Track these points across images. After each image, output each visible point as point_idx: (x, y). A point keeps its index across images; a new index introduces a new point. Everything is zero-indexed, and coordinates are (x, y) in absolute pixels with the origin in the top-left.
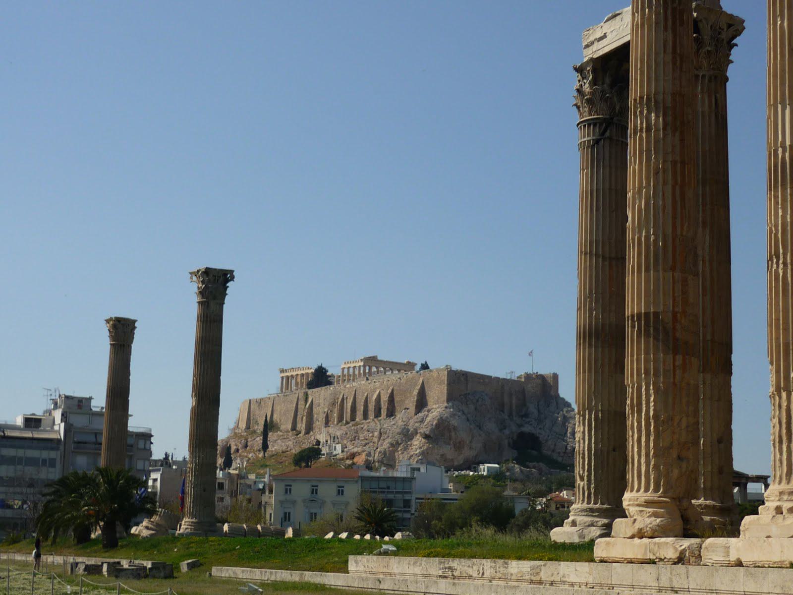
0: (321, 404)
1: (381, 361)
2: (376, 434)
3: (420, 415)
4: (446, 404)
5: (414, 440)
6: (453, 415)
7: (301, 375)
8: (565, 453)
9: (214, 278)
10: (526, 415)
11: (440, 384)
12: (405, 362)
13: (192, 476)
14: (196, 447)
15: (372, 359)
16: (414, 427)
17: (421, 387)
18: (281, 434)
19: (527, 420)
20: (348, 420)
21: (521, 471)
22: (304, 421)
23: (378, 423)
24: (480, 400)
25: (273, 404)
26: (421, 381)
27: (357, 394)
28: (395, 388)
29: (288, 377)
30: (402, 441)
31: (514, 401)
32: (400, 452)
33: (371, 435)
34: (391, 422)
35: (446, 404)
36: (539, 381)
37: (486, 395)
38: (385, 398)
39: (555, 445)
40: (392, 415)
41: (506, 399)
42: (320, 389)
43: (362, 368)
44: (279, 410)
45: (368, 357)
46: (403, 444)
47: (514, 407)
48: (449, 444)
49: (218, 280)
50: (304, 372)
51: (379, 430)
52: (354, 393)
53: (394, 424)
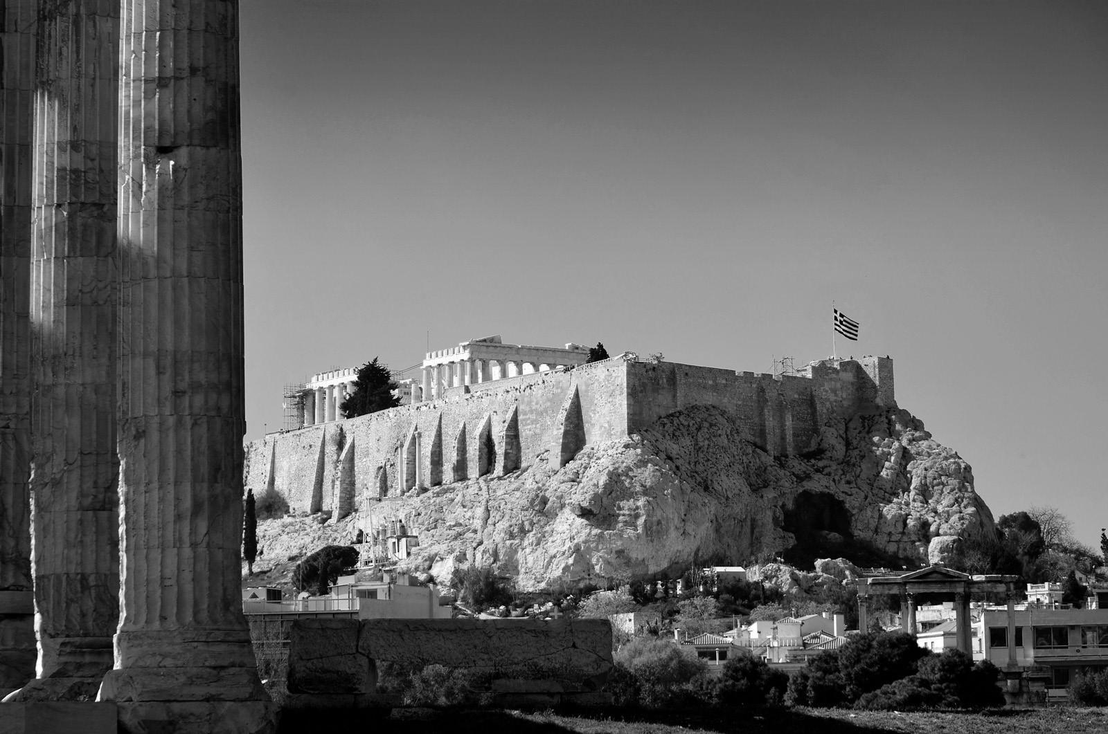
0: (371, 451)
1: (510, 348)
2: (480, 511)
3: (571, 465)
5: (558, 521)
6: (642, 463)
7: (339, 386)
8: (903, 533)
10: (819, 453)
12: (567, 346)
15: (489, 344)
16: (558, 494)
18: (290, 520)
19: (821, 464)
20: (427, 484)
21: (795, 580)
22: (337, 491)
23: (485, 488)
24: (706, 425)
25: (274, 454)
26: (571, 393)
27: (443, 426)
28: (521, 408)
30: (532, 524)
31: (789, 423)
32: (528, 550)
33: (469, 514)
34: (511, 483)
35: (626, 439)
36: (849, 376)
37: (723, 413)
38: (498, 434)
40: (517, 467)
41: (771, 423)
42: (367, 416)
43: (468, 365)
45: (480, 341)
46: (534, 532)
47: (789, 438)
51: (484, 502)
52: (437, 423)
53: (517, 489)
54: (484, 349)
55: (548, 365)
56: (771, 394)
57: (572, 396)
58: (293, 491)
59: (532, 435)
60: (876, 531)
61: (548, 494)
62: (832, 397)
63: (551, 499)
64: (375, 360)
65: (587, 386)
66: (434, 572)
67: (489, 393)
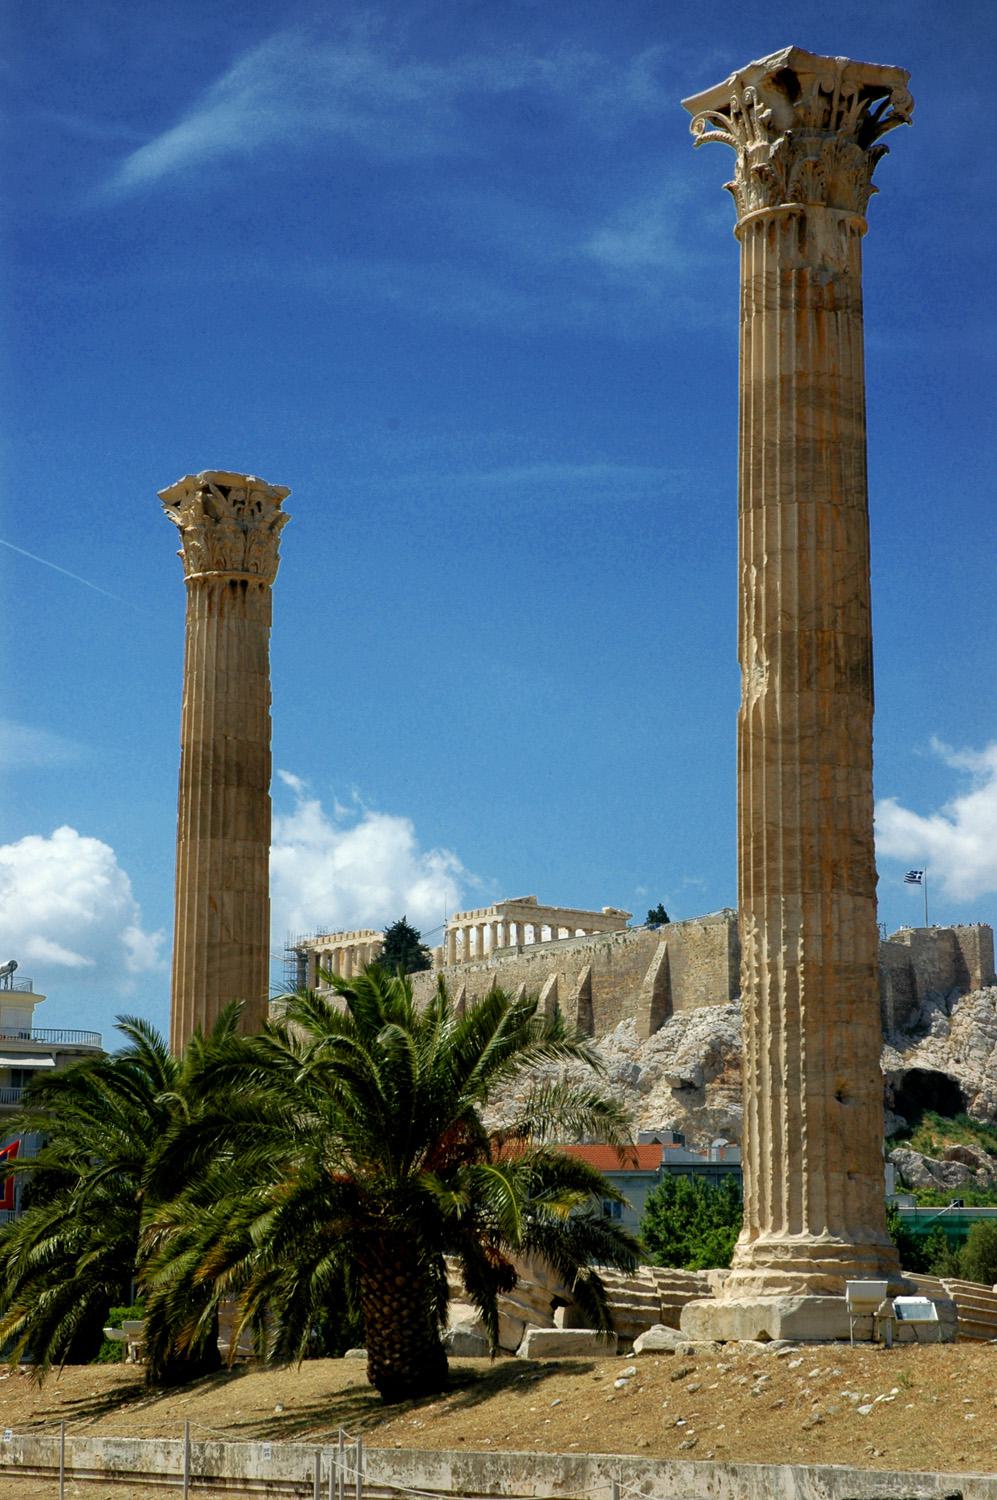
1: (546, 910)
3: (664, 1032)
4: (728, 1006)
5: (653, 1094)
7: (347, 949)
9: (822, 103)
11: (710, 954)
12: (604, 910)
13: (775, 1030)
14: (789, 888)
15: (524, 904)
16: (653, 1064)
17: (662, 963)
31: (890, 994)
36: (947, 946)
38: (570, 995)
47: (890, 1011)
49: (840, 115)
50: (356, 942)
55: (584, 930)
57: (662, 956)
59: (610, 1000)
61: (640, 1064)
63: (644, 1070)
64: (404, 919)
65: (680, 944)
67: (557, 952)
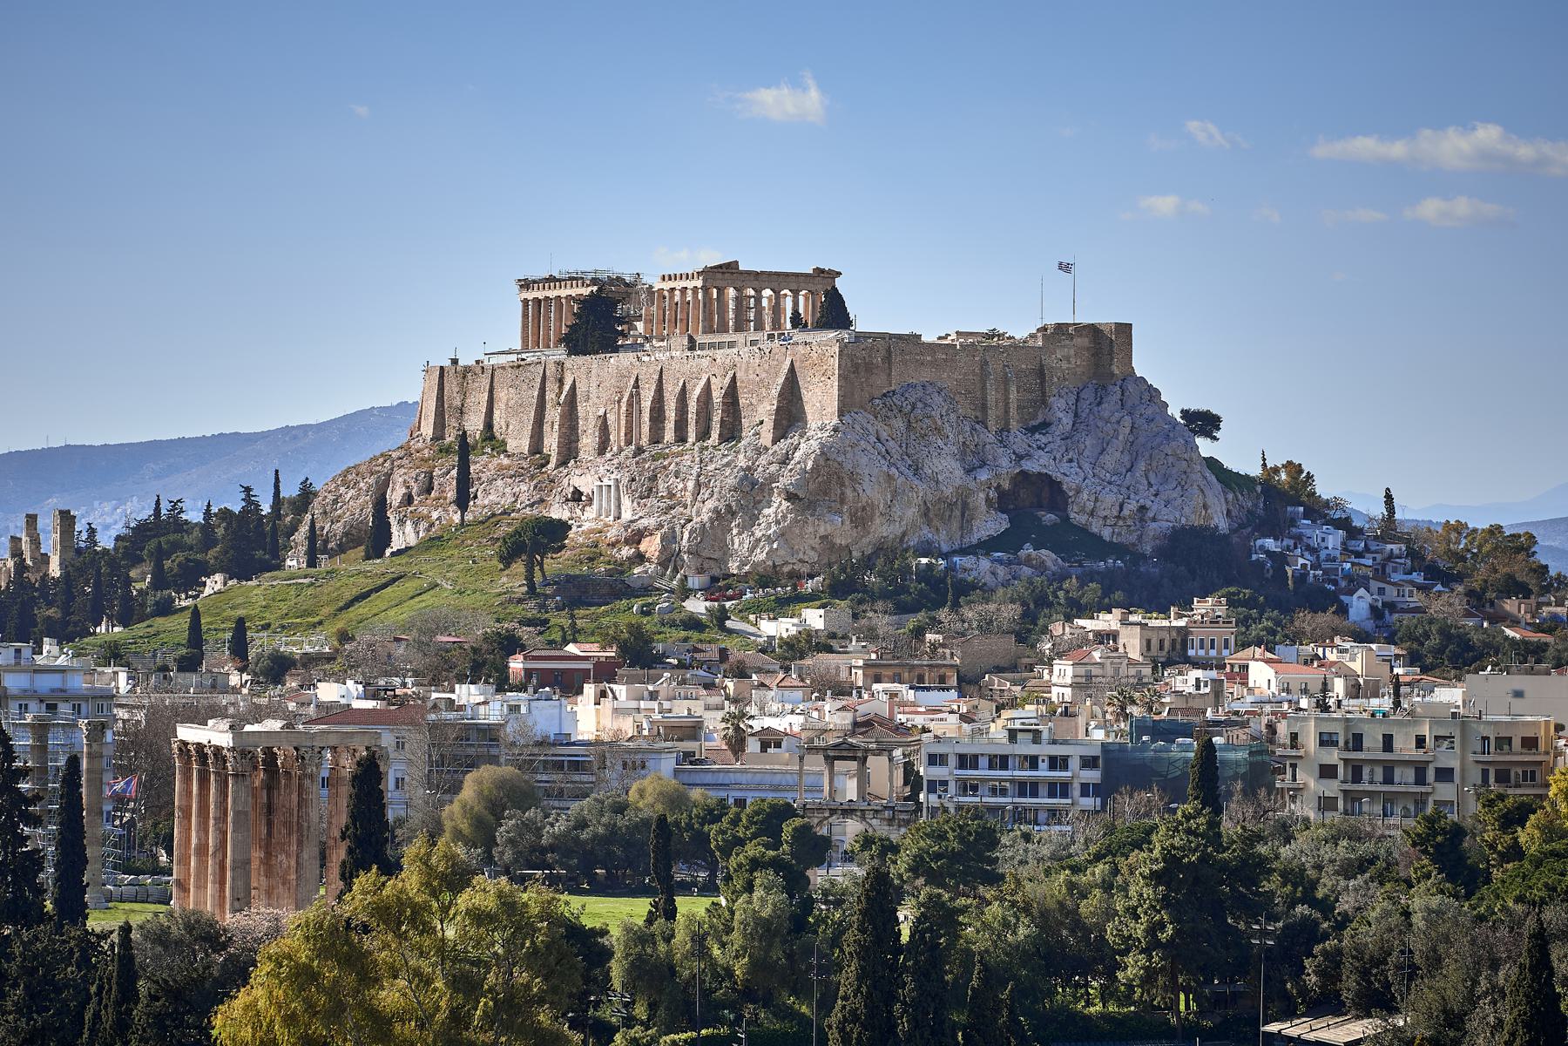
1: (749, 273)
2: (691, 485)
3: (783, 445)
7: (566, 298)
8: (1118, 517)
10: (1044, 426)
15: (724, 270)
20: (645, 441)
24: (920, 405)
25: (492, 382)
29: (537, 301)
31: (1013, 396)
36: (1083, 341)
38: (717, 396)
39: (1097, 500)
40: (733, 438)
41: (992, 396)
44: (504, 400)
45: (715, 267)
47: (1013, 411)
48: (839, 512)
53: (728, 465)
54: (719, 275)
56: (995, 367)
58: (511, 427)
60: (1092, 514)
62: (1067, 362)
66: (642, 547)
